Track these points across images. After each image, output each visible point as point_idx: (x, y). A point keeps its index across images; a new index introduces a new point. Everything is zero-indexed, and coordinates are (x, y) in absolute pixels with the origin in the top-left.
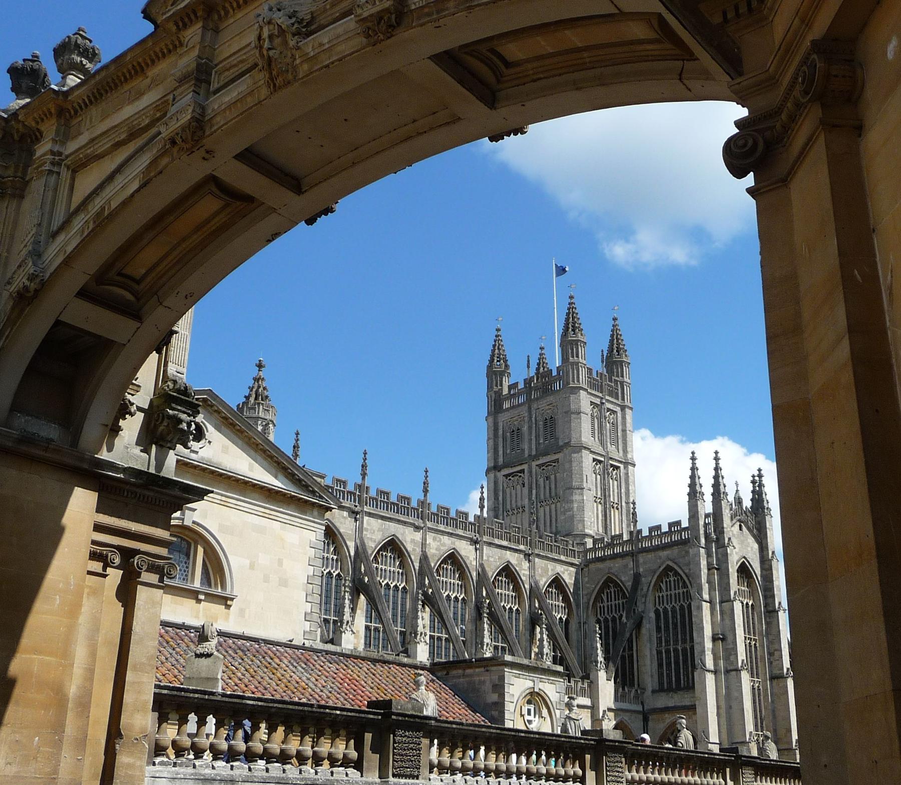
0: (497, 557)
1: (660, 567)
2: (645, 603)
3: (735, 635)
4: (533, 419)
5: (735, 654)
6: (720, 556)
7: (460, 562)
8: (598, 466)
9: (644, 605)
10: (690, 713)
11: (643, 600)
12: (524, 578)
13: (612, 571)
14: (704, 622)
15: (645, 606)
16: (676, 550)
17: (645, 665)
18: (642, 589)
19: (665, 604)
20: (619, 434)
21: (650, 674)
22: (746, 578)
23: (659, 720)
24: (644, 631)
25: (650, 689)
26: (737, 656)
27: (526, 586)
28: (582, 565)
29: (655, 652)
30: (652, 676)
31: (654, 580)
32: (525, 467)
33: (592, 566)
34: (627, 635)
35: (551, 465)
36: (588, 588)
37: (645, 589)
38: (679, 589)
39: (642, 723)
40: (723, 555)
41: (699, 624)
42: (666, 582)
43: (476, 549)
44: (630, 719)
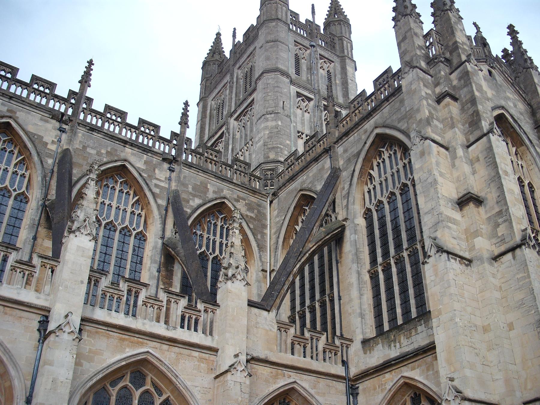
0: (103, 151)
1: (365, 143)
2: (347, 206)
3: (501, 187)
4: (235, 79)
5: (505, 221)
6: (455, 82)
7: (23, 142)
8: (305, 104)
9: (345, 210)
10: (429, 359)
11: (345, 202)
12: (157, 191)
13: (305, 186)
14: (436, 173)
15: (348, 209)
16: (386, 110)
17: (351, 300)
18: (344, 188)
19: (379, 197)
20: (337, 82)
21: (358, 311)
22: (513, 146)
23: (375, 389)
24: (347, 247)
25: (358, 338)
26: (511, 223)
27: (160, 202)
28: (271, 195)
29: (367, 277)
30: (362, 316)
31: (359, 166)
32: (224, 129)
33: (282, 194)
34: (311, 246)
35: (248, 111)
36: (277, 223)
37: (347, 186)
38: (397, 164)
39: (344, 398)
40: (460, 79)
41: (426, 181)
42: (378, 165)
43: (62, 130)
44: (314, 387)
